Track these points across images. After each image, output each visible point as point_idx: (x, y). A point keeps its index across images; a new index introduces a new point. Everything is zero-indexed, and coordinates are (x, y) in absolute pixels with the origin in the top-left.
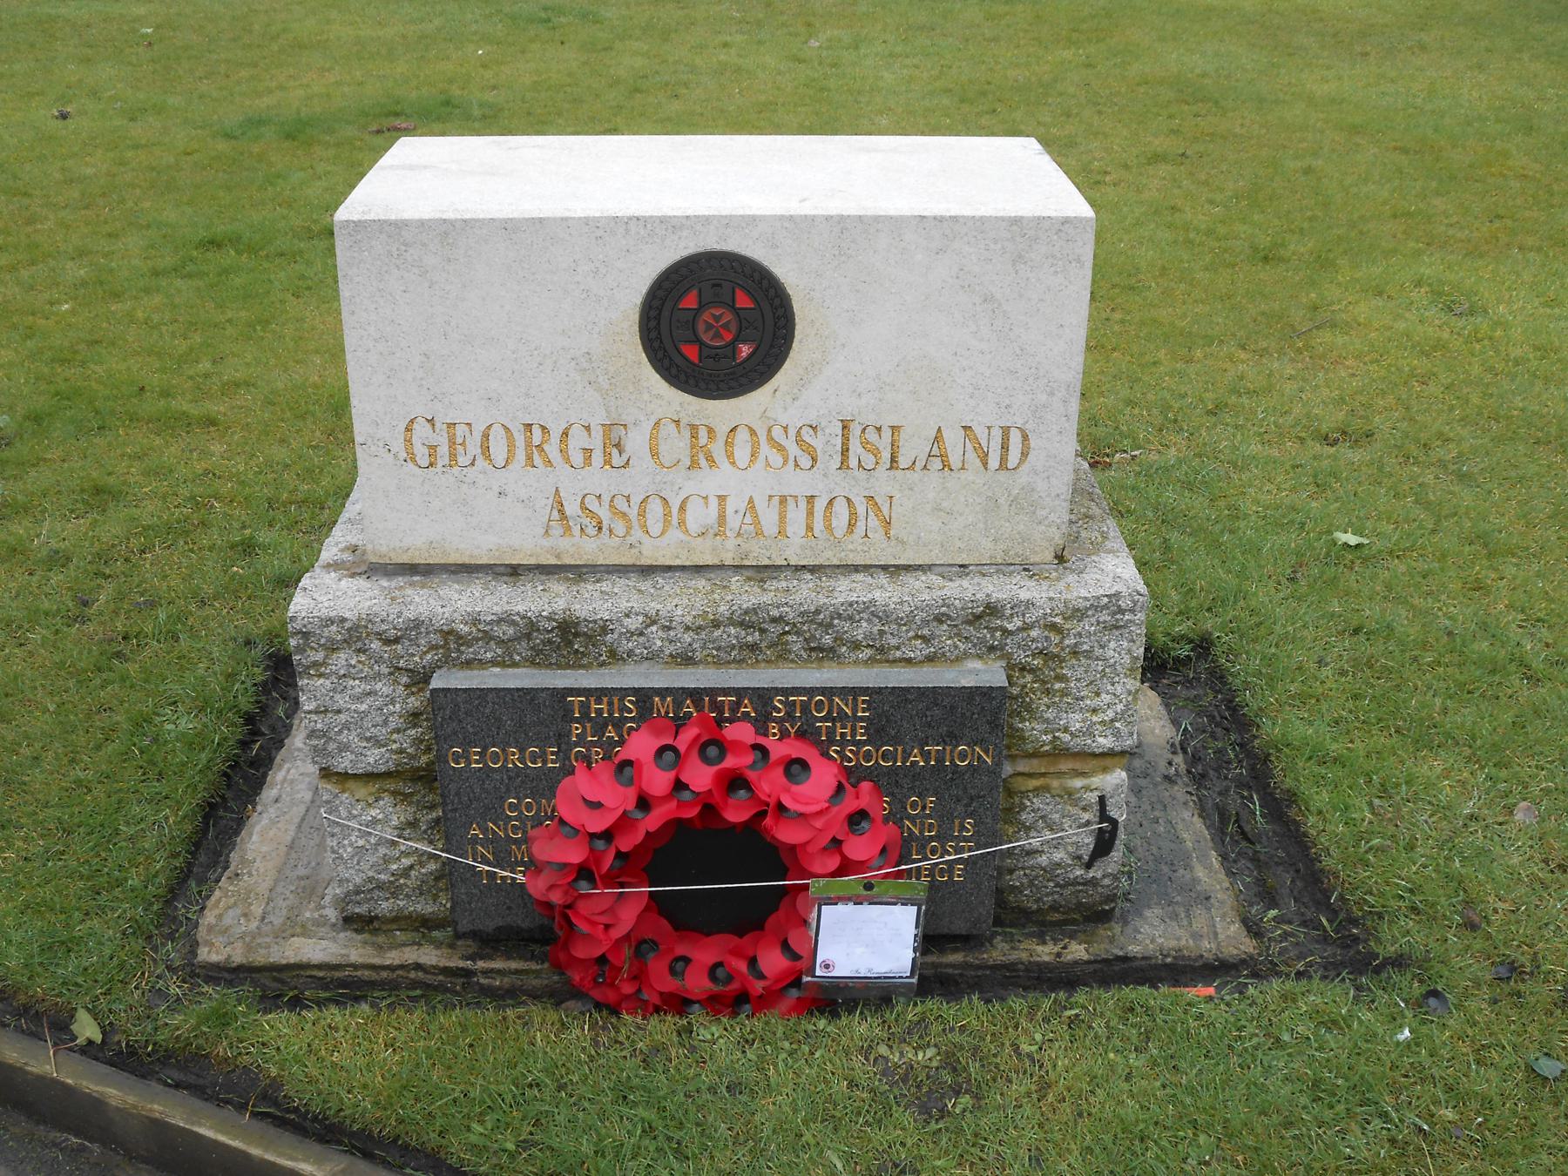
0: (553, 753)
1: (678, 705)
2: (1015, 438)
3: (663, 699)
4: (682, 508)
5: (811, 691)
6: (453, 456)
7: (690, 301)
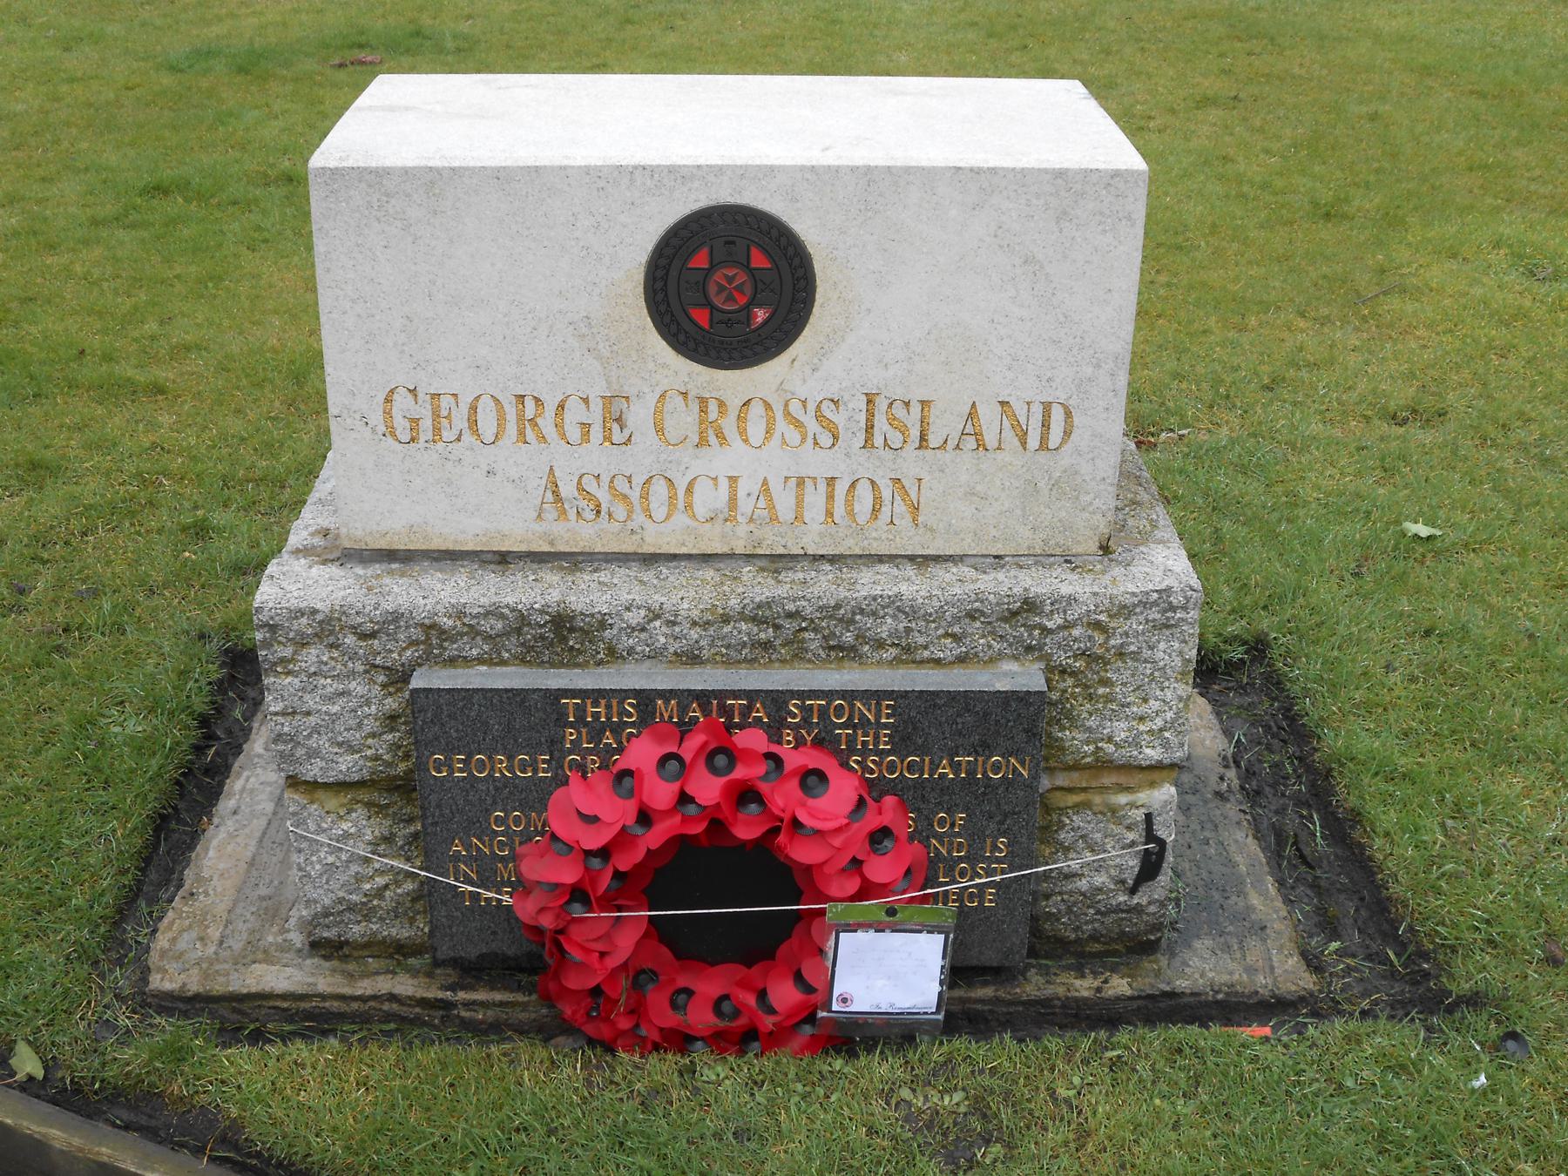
0: (544, 761)
1: (683, 709)
2: (1057, 415)
3: (667, 702)
4: (689, 490)
5: (829, 695)
6: (437, 430)
7: (700, 261)
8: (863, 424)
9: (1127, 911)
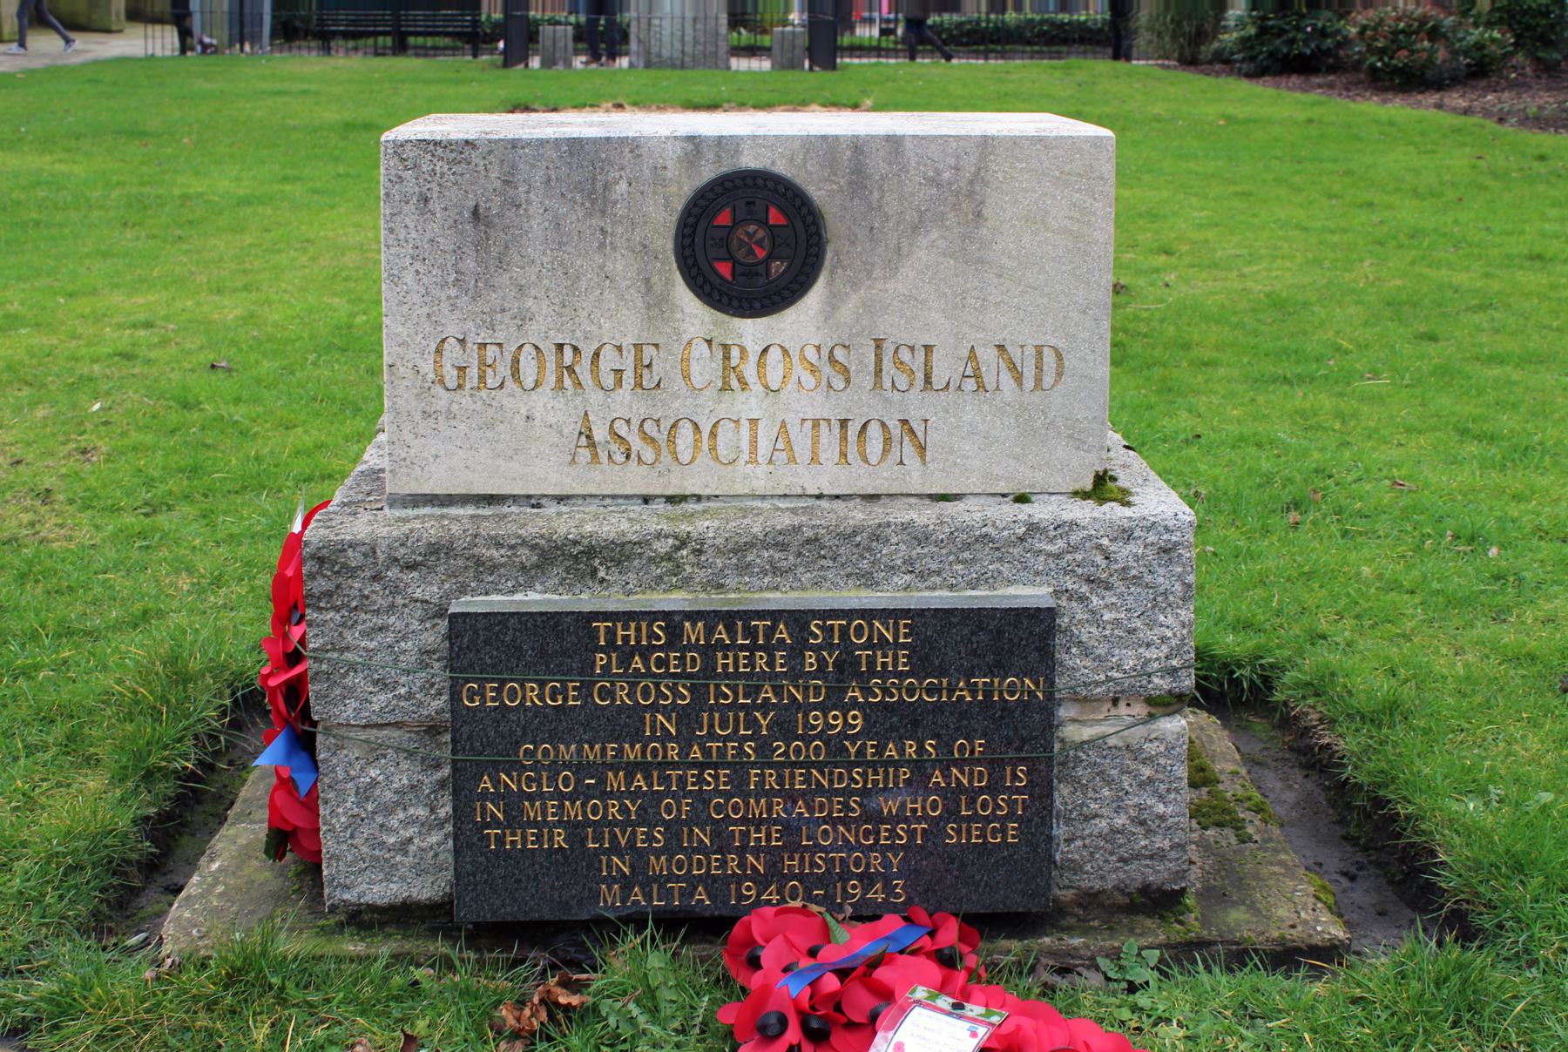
0: (575, 689)
1: (710, 630)
2: (1049, 358)
3: (694, 625)
4: (713, 434)
5: (849, 614)
6: (482, 378)
8: (872, 368)
9: (1151, 857)
